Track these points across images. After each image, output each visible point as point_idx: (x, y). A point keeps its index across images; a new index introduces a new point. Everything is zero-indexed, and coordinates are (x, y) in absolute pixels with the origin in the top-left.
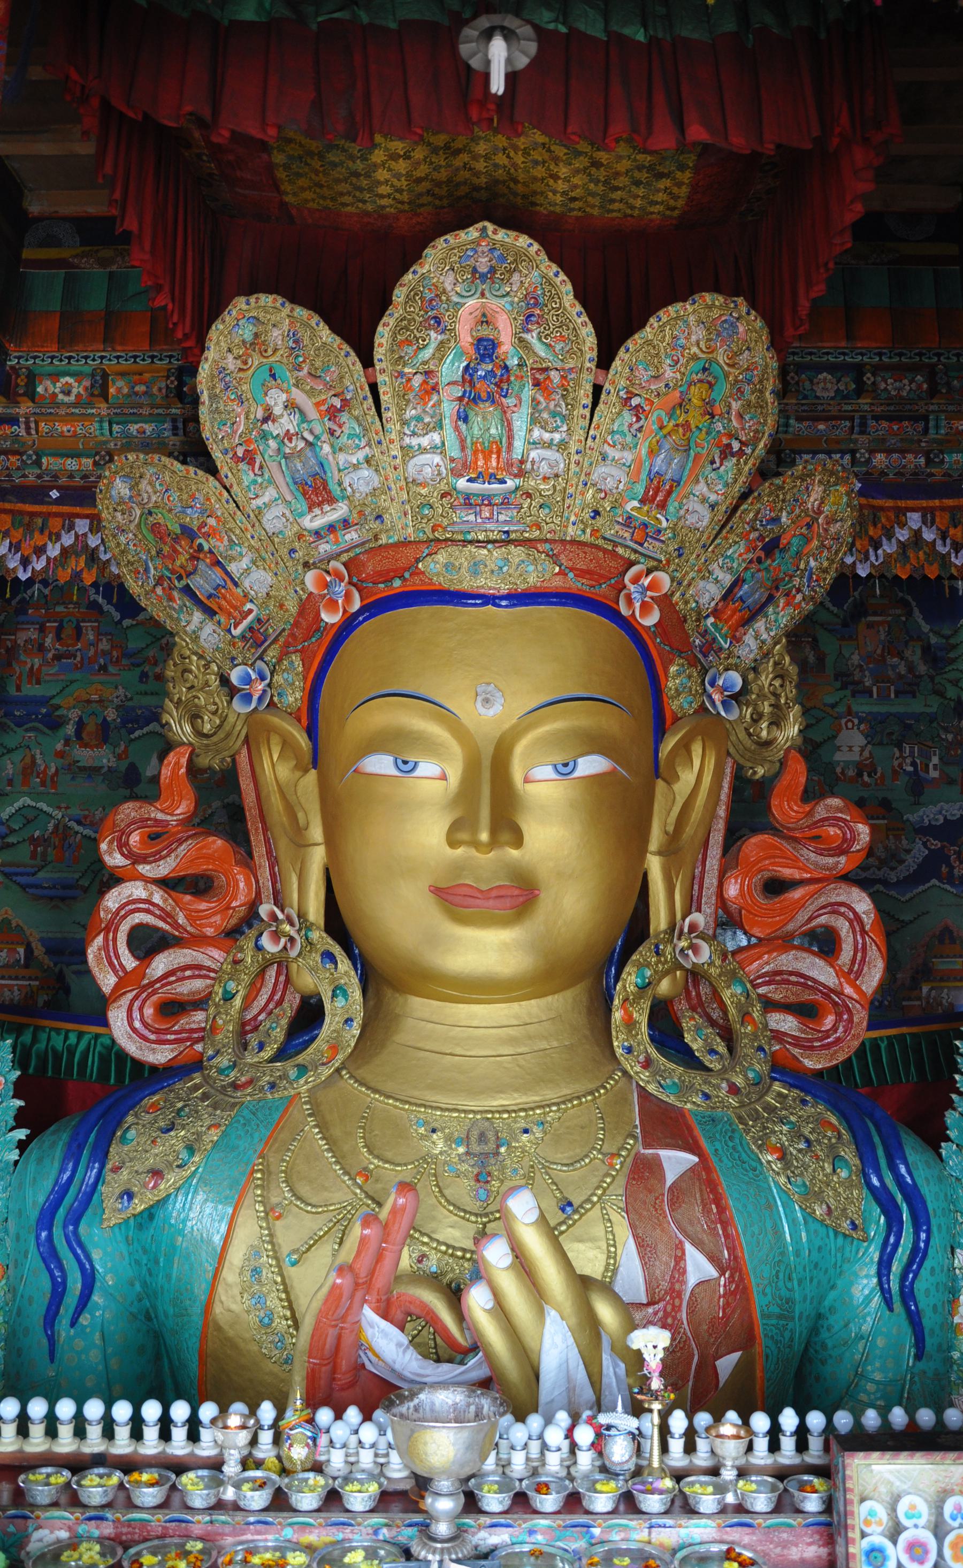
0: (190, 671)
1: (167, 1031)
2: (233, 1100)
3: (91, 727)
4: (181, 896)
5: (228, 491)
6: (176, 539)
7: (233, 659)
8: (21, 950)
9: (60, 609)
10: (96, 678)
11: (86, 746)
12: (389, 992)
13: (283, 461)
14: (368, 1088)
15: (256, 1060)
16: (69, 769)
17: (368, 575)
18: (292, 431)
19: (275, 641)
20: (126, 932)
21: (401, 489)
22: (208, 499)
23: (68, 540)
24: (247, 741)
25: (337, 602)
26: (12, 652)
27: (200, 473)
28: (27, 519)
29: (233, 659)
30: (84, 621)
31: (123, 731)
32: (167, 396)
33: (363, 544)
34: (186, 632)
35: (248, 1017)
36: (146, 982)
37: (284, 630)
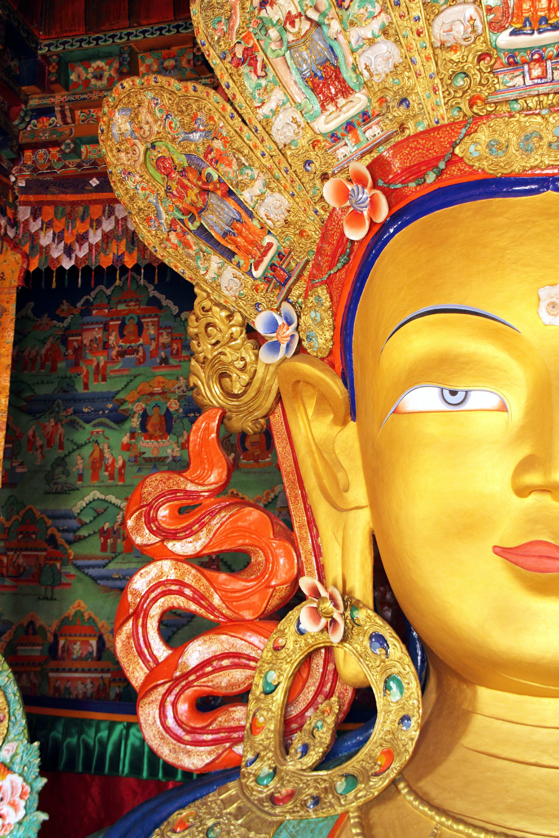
0: (214, 326)
1: (203, 730)
2: (269, 818)
3: (154, 420)
4: (215, 574)
5: (232, 105)
6: (183, 172)
7: (258, 305)
8: (94, 642)
9: (121, 307)
10: (158, 372)
11: (151, 437)
12: (454, 683)
13: (288, 54)
14: (433, 807)
15: (299, 766)
16: (136, 461)
17: (397, 175)
18: (294, 13)
19: (300, 276)
20: (157, 618)
21: (428, 59)
22: (211, 118)
23: (108, 225)
24: (279, 399)
25: (362, 215)
26: (79, 352)
27: (200, 88)
28: (68, 208)
29: (258, 305)
30: (144, 317)
31: (186, 421)
32: (195, 65)
33: (388, 139)
34: (206, 281)
35: (294, 713)
36: (178, 674)
37: (308, 262)
